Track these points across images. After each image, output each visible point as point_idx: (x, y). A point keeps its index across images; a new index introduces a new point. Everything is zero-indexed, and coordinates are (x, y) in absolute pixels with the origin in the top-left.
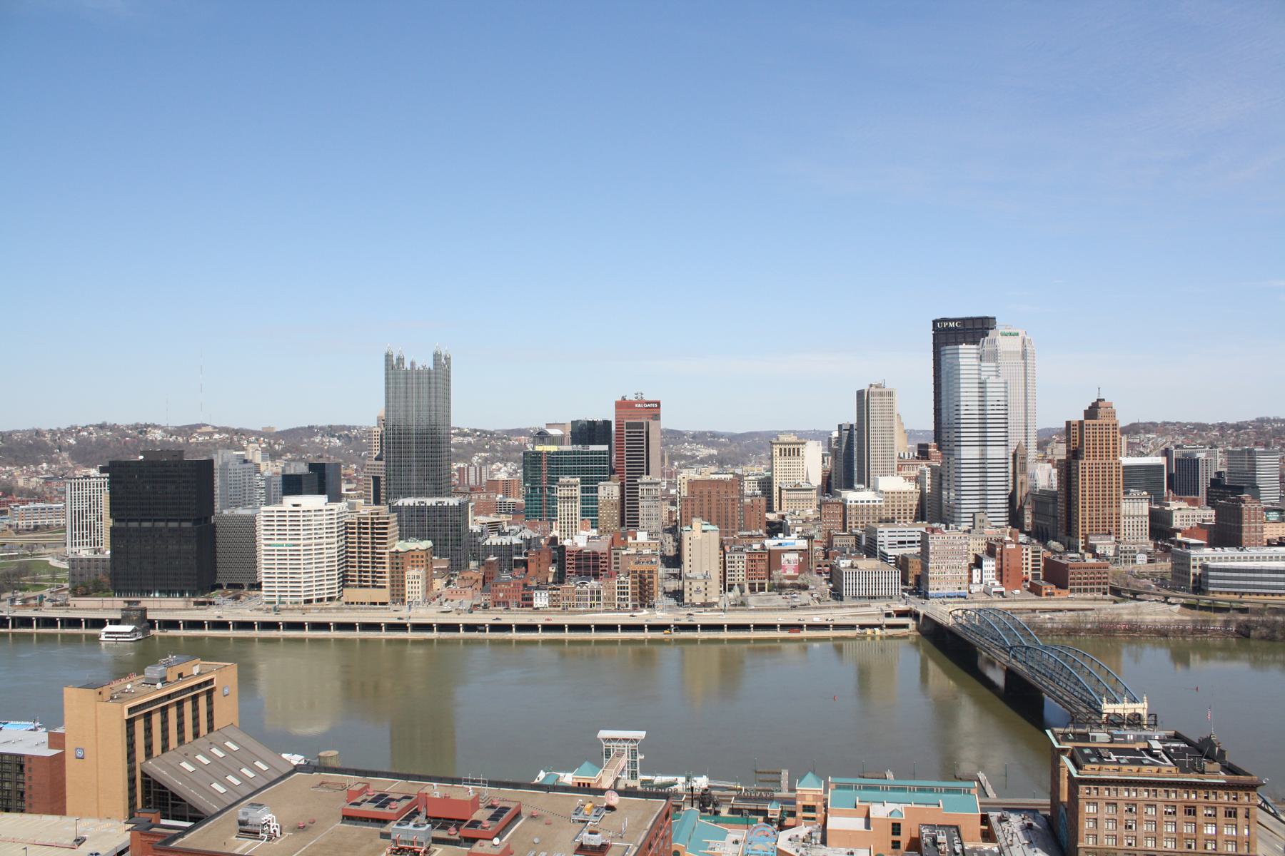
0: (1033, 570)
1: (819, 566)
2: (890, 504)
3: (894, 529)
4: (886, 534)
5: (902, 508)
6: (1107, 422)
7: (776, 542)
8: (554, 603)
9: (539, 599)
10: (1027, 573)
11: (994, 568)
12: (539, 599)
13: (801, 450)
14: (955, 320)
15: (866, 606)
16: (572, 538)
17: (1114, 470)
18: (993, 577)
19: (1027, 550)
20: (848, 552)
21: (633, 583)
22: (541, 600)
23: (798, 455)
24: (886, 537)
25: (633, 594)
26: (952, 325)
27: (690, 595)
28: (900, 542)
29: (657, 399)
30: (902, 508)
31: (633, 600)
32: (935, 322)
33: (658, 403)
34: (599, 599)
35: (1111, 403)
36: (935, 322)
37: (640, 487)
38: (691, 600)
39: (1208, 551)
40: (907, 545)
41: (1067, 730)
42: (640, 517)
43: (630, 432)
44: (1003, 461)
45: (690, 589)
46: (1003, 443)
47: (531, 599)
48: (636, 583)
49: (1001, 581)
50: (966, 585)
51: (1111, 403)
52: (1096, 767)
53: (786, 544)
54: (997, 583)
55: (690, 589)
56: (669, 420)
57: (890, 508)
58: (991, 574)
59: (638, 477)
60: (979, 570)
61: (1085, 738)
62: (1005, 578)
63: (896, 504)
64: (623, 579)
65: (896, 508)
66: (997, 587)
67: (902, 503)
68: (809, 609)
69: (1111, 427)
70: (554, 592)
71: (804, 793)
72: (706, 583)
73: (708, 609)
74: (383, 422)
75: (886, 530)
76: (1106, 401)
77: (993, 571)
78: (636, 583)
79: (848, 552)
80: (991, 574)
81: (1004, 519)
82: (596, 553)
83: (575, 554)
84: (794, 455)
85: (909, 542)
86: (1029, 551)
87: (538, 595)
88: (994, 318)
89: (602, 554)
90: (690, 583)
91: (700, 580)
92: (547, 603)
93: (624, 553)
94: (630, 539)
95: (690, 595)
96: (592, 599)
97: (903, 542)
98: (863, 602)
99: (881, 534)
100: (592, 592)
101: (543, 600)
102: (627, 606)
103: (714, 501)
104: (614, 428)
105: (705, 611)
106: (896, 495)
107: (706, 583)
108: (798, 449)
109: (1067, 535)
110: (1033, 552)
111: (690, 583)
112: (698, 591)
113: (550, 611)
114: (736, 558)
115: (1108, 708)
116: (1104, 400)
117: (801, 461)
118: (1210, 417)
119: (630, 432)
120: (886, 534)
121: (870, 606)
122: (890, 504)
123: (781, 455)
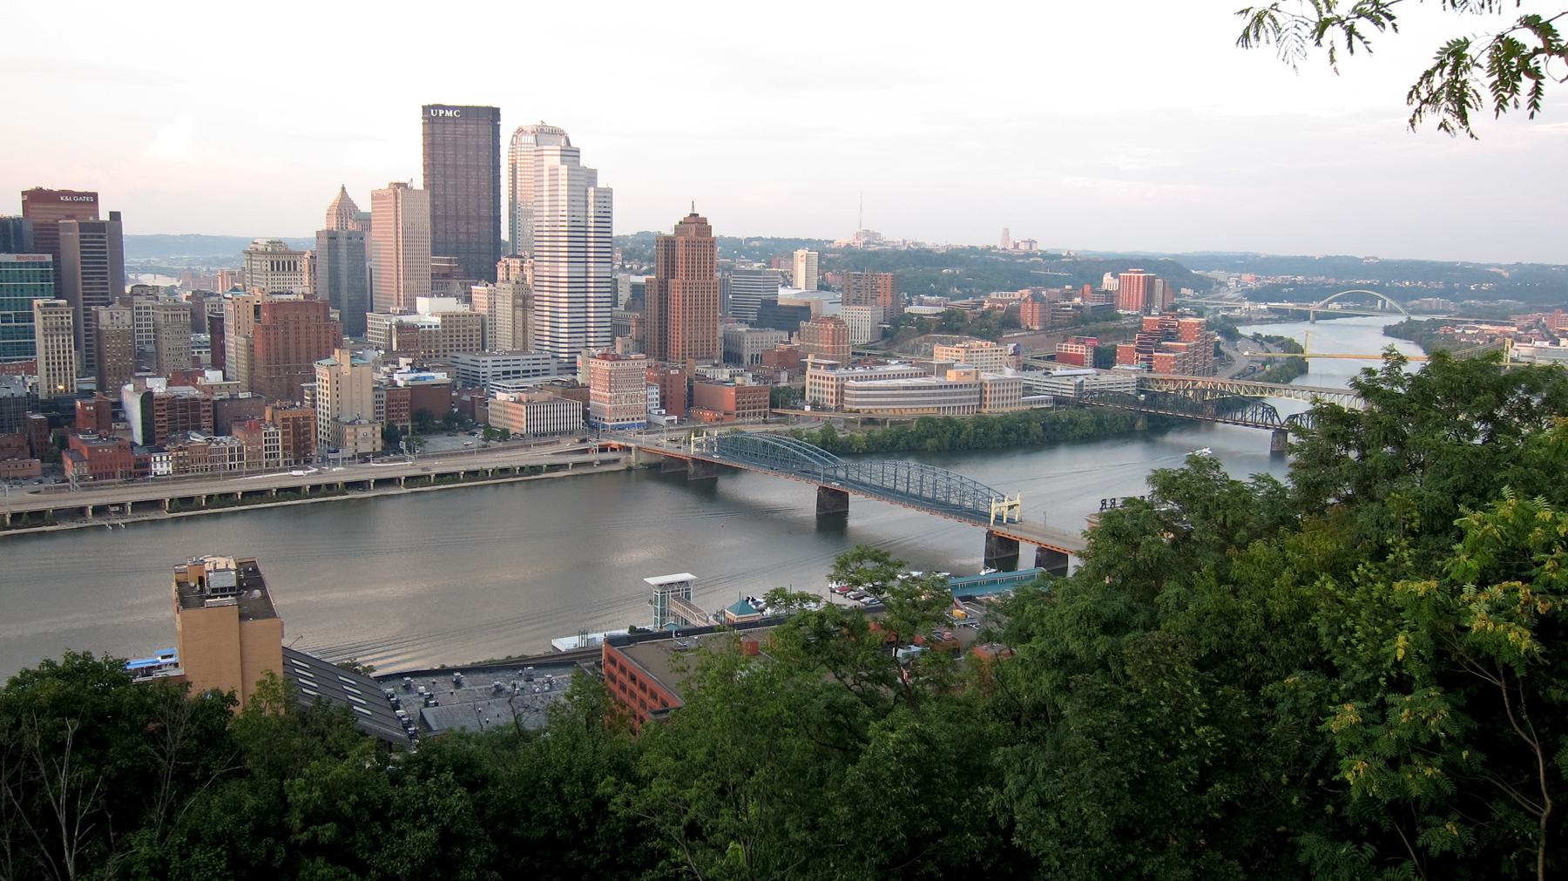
3: (528, 357)
4: (489, 363)
5: (461, 334)
6: (705, 239)
8: (182, 470)
9: (158, 465)
11: (658, 396)
12: (158, 465)
13: (298, 263)
14: (453, 108)
17: (712, 290)
21: (284, 434)
22: (162, 465)
23: (295, 269)
24: (490, 367)
25: (285, 448)
26: (449, 113)
27: (356, 444)
28: (504, 373)
30: (461, 334)
31: (285, 456)
32: (426, 109)
33: (95, 195)
34: (241, 458)
36: (426, 109)
39: (842, 370)
40: (512, 375)
45: (356, 437)
48: (288, 433)
55: (356, 437)
57: (448, 334)
58: (655, 402)
62: (668, 405)
63: (454, 329)
65: (455, 334)
67: (461, 328)
70: (181, 453)
74: (715, 238)
78: (288, 433)
80: (655, 402)
82: (196, 399)
83: (166, 402)
85: (514, 372)
87: (158, 459)
88: (498, 109)
90: (355, 430)
91: (365, 425)
92: (170, 469)
95: (356, 444)
96: (232, 458)
97: (508, 373)
99: (484, 364)
100: (232, 450)
101: (165, 465)
102: (278, 465)
103: (303, 330)
105: (382, 462)
106: (454, 319)
108: (295, 263)
111: (355, 430)
112: (365, 439)
118: (1504, 263)
120: (489, 363)
121: (558, 442)
122: (448, 329)
123: (272, 269)
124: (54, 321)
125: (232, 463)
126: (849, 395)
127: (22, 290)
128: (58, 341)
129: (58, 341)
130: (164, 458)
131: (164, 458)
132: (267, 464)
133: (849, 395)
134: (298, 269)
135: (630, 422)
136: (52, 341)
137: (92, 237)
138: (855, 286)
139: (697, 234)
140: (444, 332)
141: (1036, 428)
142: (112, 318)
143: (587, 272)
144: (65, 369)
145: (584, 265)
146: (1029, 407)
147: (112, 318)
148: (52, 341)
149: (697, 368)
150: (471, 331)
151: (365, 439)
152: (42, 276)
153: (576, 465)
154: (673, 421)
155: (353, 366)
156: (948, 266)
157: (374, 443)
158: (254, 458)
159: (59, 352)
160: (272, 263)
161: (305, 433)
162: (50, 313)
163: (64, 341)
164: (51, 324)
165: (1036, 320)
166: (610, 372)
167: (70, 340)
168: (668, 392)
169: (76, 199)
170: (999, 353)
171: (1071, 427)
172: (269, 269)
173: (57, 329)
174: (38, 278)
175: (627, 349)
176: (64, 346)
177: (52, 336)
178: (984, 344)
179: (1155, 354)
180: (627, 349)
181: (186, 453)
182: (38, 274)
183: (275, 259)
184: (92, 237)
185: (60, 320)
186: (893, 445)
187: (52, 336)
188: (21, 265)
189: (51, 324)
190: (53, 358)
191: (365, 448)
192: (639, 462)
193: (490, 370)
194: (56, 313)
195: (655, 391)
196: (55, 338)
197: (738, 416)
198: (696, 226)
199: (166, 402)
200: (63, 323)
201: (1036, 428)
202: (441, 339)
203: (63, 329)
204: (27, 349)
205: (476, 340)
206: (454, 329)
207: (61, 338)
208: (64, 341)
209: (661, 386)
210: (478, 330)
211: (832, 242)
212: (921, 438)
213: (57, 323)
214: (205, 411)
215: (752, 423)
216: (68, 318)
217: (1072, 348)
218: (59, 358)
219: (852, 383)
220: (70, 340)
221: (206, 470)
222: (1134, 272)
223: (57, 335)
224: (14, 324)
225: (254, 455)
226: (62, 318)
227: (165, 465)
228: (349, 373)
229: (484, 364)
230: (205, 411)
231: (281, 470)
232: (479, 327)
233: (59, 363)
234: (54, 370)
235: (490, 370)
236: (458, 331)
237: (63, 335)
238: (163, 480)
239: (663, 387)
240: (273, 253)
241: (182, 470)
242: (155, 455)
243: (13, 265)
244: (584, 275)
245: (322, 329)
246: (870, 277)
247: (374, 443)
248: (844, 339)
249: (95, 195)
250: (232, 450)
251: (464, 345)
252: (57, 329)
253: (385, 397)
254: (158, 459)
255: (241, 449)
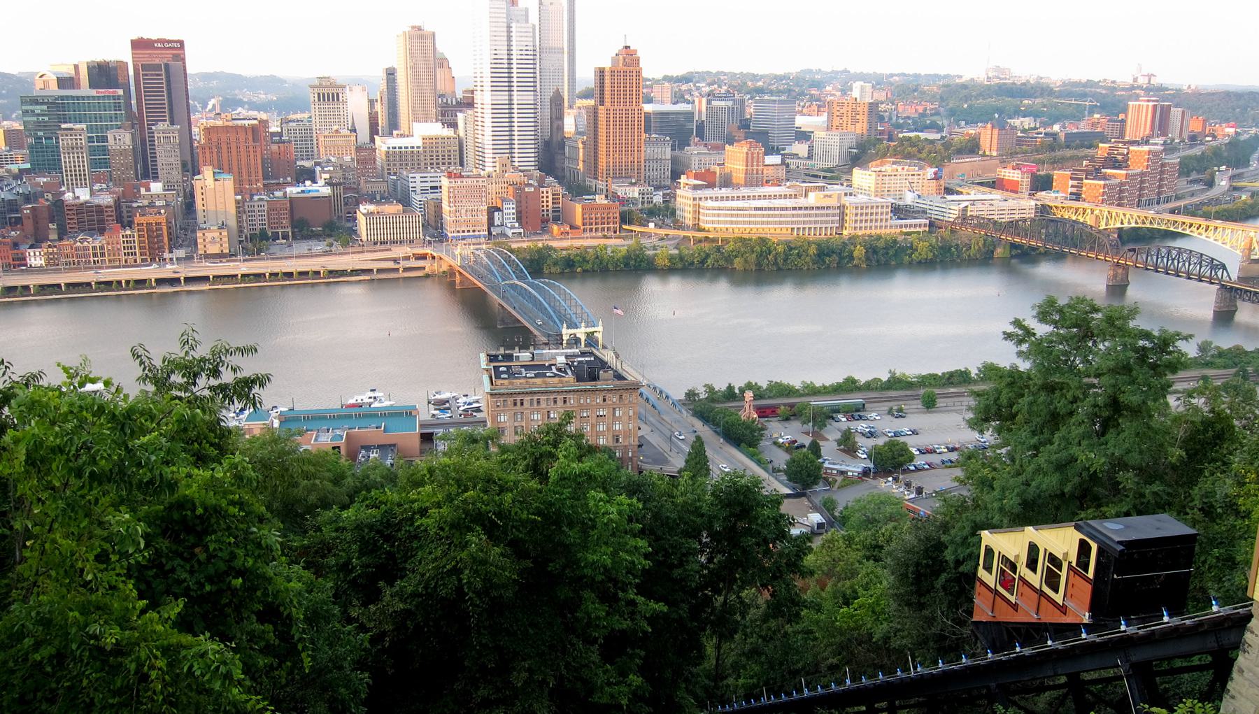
0: (553, 211)
1: (349, 213)
2: (428, 150)
4: (418, 179)
7: (299, 189)
8: (53, 264)
9: (33, 259)
10: (548, 215)
11: (514, 211)
12: (33, 259)
13: (340, 95)
15: (387, 250)
16: (74, 193)
18: (513, 219)
19: (547, 192)
20: (378, 198)
21: (139, 236)
23: (338, 100)
27: (205, 246)
28: (432, 188)
29: (180, 39)
33: (181, 43)
34: (103, 255)
35: (636, 51)
37: (156, 135)
38: (205, 252)
41: (498, 353)
42: (159, 167)
43: (146, 75)
44: (532, 106)
45: (204, 240)
46: (532, 89)
47: (25, 259)
49: (520, 223)
50: (486, 227)
51: (636, 51)
52: (506, 382)
53: (310, 191)
54: (517, 225)
55: (204, 240)
56: (195, 64)
57: (428, 154)
58: (512, 216)
59: (153, 125)
60: (500, 213)
61: (509, 358)
62: (524, 220)
64: (128, 232)
65: (434, 154)
66: (515, 228)
67: (440, 149)
68: (329, 255)
69: (634, 74)
70: (50, 250)
71: (251, 427)
72: (221, 234)
73: (224, 260)
75: (418, 176)
76: (632, 48)
77: (513, 214)
79: (378, 198)
80: (512, 216)
81: (533, 164)
84: (333, 100)
86: (550, 194)
87: (32, 254)
89: (107, 207)
90: (204, 234)
91: (213, 231)
92: (43, 262)
93: (135, 205)
94: (143, 191)
95: (205, 246)
96: (95, 255)
98: (388, 246)
99: (413, 180)
101: (38, 259)
102: (135, 261)
104: (131, 72)
105: (221, 262)
106: (434, 141)
107: (221, 234)
108: (338, 94)
109: (595, 178)
110: (553, 195)
111: (204, 234)
112: (213, 241)
113: (47, 270)
114: (256, 207)
115: (566, 333)
116: (629, 47)
117: (341, 106)
119: (146, 75)
120: (418, 179)
122: (428, 150)
123: (319, 100)
124: (70, 142)
125: (96, 259)
126: (704, 214)
127: (101, 118)
128: (74, 157)
129: (74, 157)
130: (37, 254)
131: (37, 254)
132: (126, 261)
133: (704, 214)
134: (341, 100)
135: (471, 233)
136: (69, 157)
137: (152, 75)
138: (838, 113)
139: (625, 64)
140: (425, 152)
141: (859, 251)
142: (115, 139)
143: (511, 100)
144: (81, 180)
145: (507, 93)
146: (898, 230)
147: (115, 139)
148: (69, 157)
149: (614, 186)
150: (449, 151)
151: (213, 241)
152: (115, 106)
153: (379, 271)
154: (521, 233)
155: (216, 180)
156: (1029, 96)
157: (221, 245)
158: (114, 255)
159: (75, 166)
160: (319, 95)
161: (158, 236)
162: (67, 135)
163: (78, 157)
164: (68, 144)
165: (995, 147)
166: (449, 188)
167: (83, 157)
168: (523, 208)
169: (167, 45)
170: (916, 177)
171: (909, 251)
172: (316, 100)
173: (73, 148)
174: (112, 108)
175: (504, 168)
176: (79, 162)
177: (69, 153)
178: (900, 168)
179: (1085, 181)
180: (504, 168)
181: (55, 249)
182: (112, 105)
183: (321, 92)
184: (152, 75)
185: (70, 142)
186: (703, 262)
187: (69, 153)
188: (99, 98)
189: (68, 144)
190: (71, 171)
191: (213, 249)
192: (441, 270)
193: (419, 186)
194: (71, 135)
195: (511, 206)
196: (71, 155)
197: (584, 230)
198: (629, 57)
199: (75, 208)
200: (77, 144)
201: (859, 251)
202: (422, 158)
203: (77, 148)
204: (55, 164)
205: (455, 158)
206: (434, 149)
207: (76, 155)
208: (78, 157)
209: (517, 202)
210: (455, 151)
211: (961, 77)
212: (729, 259)
213: (72, 144)
214: (108, 216)
215: (594, 238)
216: (81, 139)
217: (1010, 174)
218: (75, 171)
219: (710, 204)
220: (83, 157)
221: (74, 264)
222: (1144, 101)
223: (73, 153)
224: (96, 144)
225: (114, 252)
226: (76, 139)
227: (38, 259)
228: (212, 186)
229: (413, 180)
230: (108, 216)
231: (137, 266)
232: (457, 148)
233: (76, 175)
234: (72, 180)
235: (419, 186)
236: (437, 152)
237: (78, 153)
238: (37, 271)
239: (519, 203)
240: (320, 86)
241: (53, 264)
242: (29, 250)
243: (93, 98)
244: (507, 102)
245: (251, 149)
246: (850, 104)
247: (221, 245)
248: (758, 161)
249: (181, 43)
250: (94, 248)
251: (438, 164)
252: (73, 148)
253: (266, 207)
254: (32, 254)
255: (102, 248)
